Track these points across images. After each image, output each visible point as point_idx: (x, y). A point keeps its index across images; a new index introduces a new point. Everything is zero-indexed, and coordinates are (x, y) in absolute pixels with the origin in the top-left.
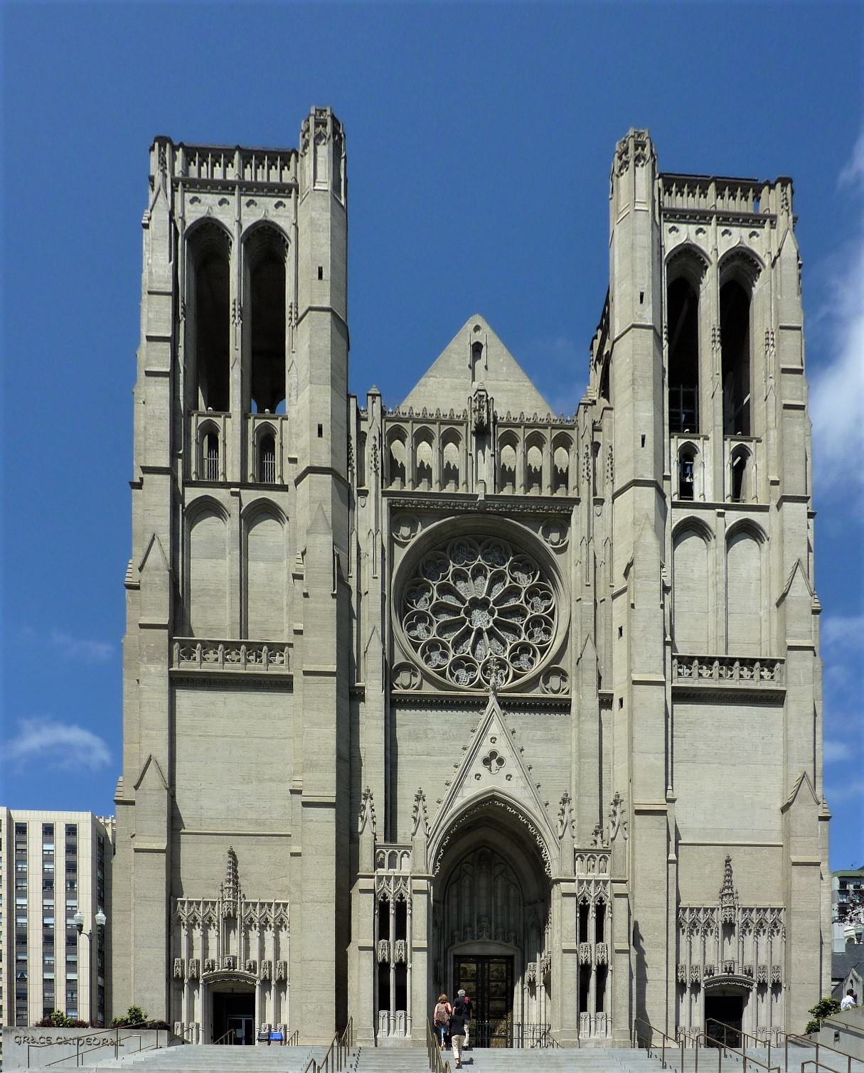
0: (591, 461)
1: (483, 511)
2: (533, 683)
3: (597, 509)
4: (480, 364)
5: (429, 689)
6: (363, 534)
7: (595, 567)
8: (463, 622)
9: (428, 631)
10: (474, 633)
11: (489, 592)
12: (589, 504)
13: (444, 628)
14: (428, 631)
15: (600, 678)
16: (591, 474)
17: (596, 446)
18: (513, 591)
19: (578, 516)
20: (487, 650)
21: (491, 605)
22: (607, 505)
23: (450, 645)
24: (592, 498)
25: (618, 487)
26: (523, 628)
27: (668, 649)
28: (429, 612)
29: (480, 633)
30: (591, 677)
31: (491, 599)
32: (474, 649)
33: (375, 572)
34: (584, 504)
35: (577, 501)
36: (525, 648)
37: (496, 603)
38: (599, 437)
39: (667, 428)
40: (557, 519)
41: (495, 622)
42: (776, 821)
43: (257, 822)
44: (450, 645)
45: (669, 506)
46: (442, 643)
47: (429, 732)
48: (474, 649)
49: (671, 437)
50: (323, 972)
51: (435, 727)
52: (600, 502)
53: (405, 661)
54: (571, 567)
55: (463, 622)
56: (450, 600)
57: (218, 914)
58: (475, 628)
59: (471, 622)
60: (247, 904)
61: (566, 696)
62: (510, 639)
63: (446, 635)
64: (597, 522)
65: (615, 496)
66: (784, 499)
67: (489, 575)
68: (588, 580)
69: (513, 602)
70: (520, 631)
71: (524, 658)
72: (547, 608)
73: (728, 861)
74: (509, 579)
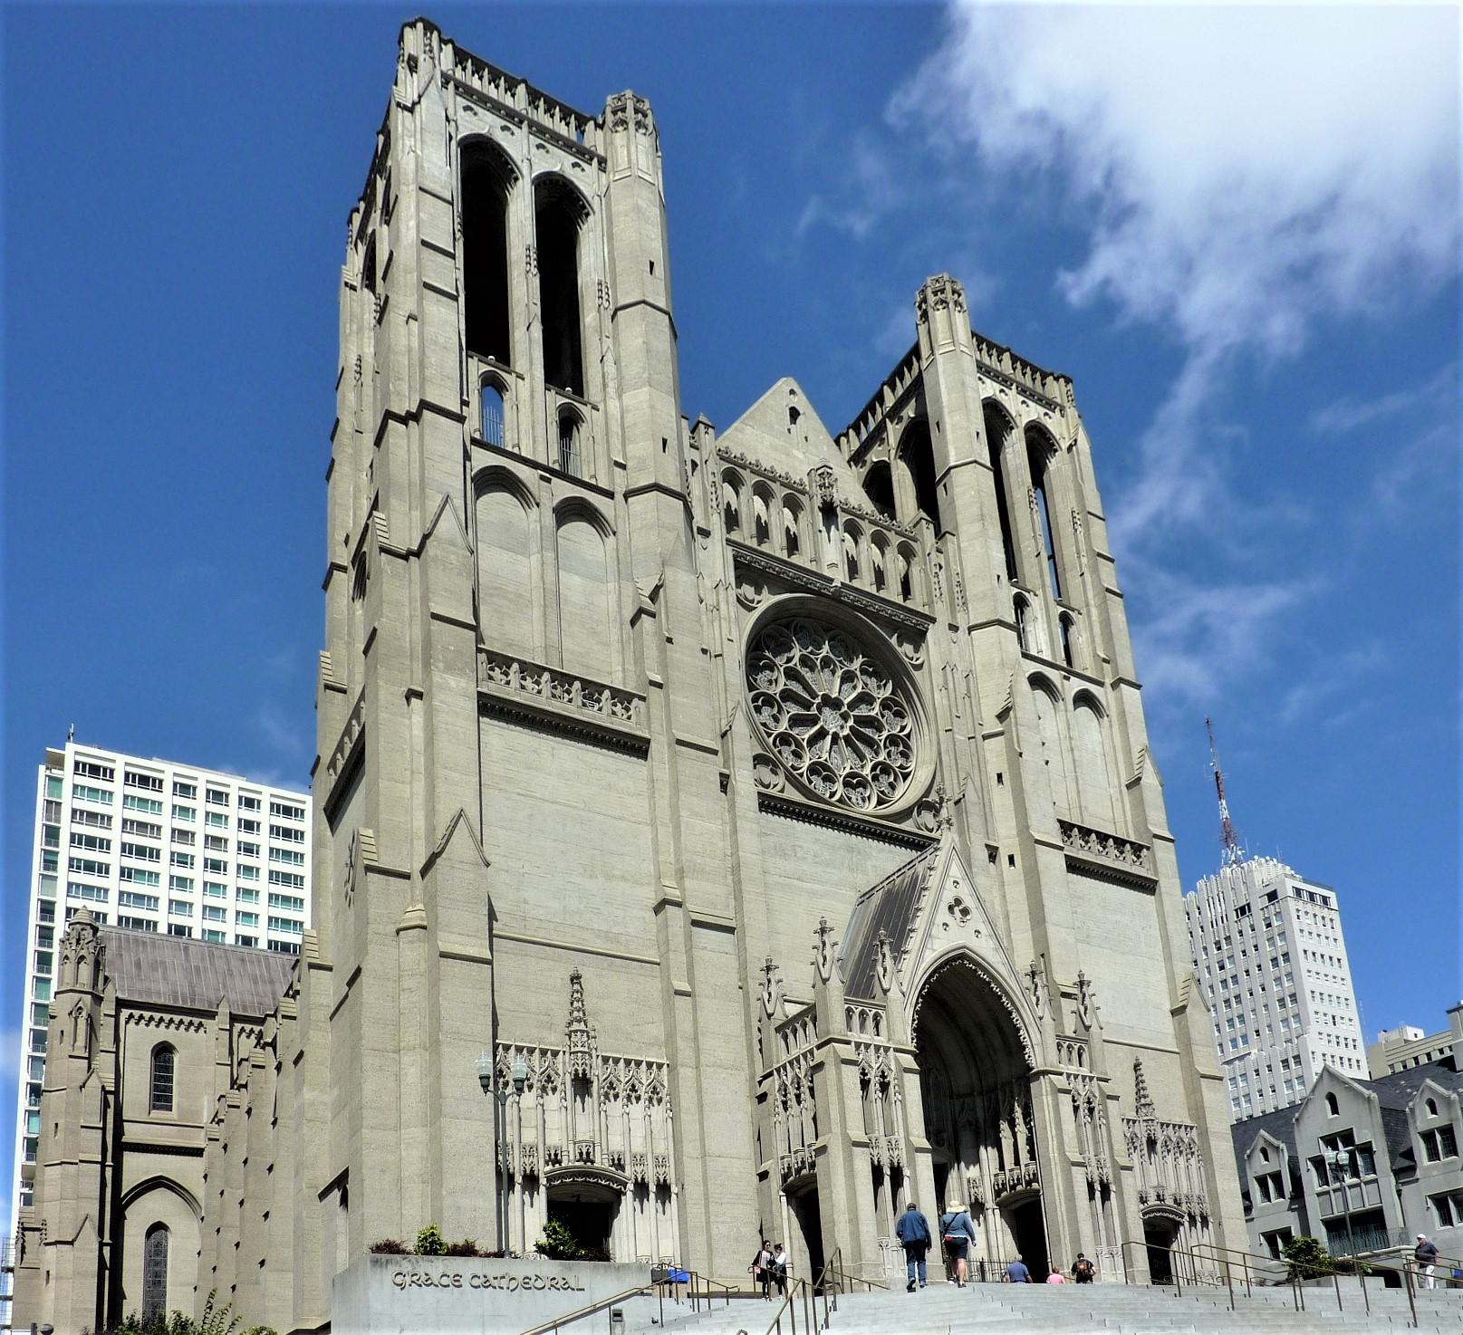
2: (905, 814)
5: (792, 794)
9: (777, 720)
10: (829, 738)
13: (796, 721)
14: (777, 720)
18: (865, 699)
20: (844, 763)
21: (845, 709)
23: (805, 744)
26: (882, 744)
28: (777, 697)
31: (846, 702)
42: (1168, 1024)
43: (607, 936)
44: (805, 744)
46: (795, 740)
47: (798, 850)
50: (736, 1175)
51: (805, 845)
53: (761, 752)
56: (795, 687)
57: (564, 1069)
58: (831, 732)
60: (606, 1060)
70: (879, 746)
73: (1137, 1067)
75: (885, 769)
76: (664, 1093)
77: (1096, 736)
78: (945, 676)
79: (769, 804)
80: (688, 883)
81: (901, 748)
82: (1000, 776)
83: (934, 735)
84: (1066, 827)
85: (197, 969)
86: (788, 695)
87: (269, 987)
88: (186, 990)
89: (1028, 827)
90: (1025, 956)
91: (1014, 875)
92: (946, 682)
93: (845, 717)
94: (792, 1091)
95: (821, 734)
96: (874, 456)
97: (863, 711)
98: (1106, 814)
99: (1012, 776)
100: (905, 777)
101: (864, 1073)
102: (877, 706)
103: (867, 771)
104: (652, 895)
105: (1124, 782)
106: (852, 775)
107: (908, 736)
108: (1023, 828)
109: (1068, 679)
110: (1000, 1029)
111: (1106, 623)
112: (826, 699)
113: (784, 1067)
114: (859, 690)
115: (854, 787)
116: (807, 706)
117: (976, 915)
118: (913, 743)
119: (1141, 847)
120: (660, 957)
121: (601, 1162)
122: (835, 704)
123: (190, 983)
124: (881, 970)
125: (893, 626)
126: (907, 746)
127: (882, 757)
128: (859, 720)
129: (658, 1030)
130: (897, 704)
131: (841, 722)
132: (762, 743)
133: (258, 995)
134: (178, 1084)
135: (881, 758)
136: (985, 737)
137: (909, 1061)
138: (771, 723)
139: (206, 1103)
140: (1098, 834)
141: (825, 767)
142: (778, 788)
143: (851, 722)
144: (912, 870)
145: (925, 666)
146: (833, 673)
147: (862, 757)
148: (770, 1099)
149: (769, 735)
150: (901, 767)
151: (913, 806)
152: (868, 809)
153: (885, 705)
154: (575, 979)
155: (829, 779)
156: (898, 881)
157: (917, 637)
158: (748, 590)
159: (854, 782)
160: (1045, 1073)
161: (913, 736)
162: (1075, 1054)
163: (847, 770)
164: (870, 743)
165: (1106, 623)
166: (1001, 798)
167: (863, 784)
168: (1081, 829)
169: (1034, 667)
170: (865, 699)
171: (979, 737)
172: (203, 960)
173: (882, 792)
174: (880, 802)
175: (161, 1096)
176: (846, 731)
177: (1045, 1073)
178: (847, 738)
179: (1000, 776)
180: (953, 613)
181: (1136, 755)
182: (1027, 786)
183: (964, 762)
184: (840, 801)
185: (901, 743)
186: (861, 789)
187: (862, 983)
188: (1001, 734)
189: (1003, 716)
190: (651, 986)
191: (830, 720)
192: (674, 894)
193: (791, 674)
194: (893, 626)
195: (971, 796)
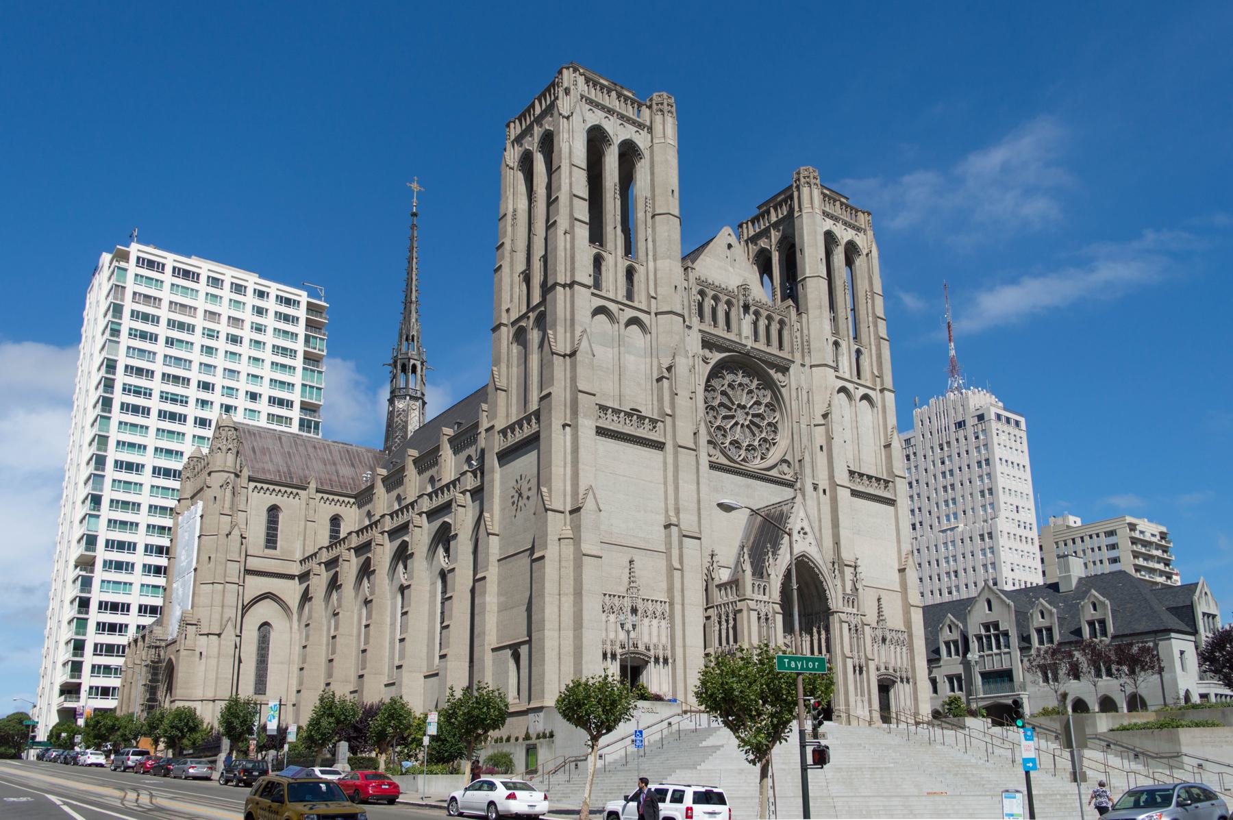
9: (715, 417)
10: (739, 426)
41: (751, 421)
58: (741, 423)
60: (643, 600)
75: (765, 440)
76: (666, 615)
77: (870, 417)
78: (798, 393)
79: (714, 466)
80: (681, 516)
81: (773, 429)
82: (821, 447)
83: (790, 424)
84: (852, 473)
85: (289, 453)
86: (721, 404)
87: (333, 467)
88: (286, 470)
89: (833, 477)
90: (830, 556)
91: (825, 500)
92: (798, 397)
93: (747, 414)
94: (724, 618)
95: (736, 424)
96: (763, 243)
98: (872, 464)
99: (828, 448)
100: (774, 444)
101: (759, 614)
102: (763, 407)
103: (756, 443)
104: (664, 519)
105: (883, 444)
106: (749, 446)
107: (776, 422)
108: (831, 477)
109: (858, 389)
110: (816, 587)
111: (879, 356)
112: (739, 406)
113: (720, 605)
114: (755, 399)
116: (730, 409)
117: (810, 535)
118: (779, 426)
119: (887, 482)
120: (666, 549)
121: (641, 648)
122: (744, 407)
123: (287, 464)
124: (767, 564)
125: (772, 365)
126: (776, 428)
128: (754, 416)
129: (664, 585)
130: (772, 405)
131: (745, 416)
132: (709, 433)
133: (328, 473)
134: (282, 532)
135: (763, 436)
136: (815, 425)
137: (778, 608)
138: (713, 420)
139: (299, 546)
140: (868, 476)
141: (736, 442)
142: (716, 457)
143: (750, 417)
144: (780, 508)
145: (788, 386)
146: (743, 390)
147: (754, 435)
148: (712, 619)
149: (712, 427)
150: (773, 439)
152: (756, 464)
154: (631, 562)
155: (739, 448)
156: (773, 511)
157: (784, 370)
158: (707, 352)
159: (751, 448)
160: (836, 612)
161: (779, 423)
162: (851, 602)
163: (747, 443)
164: (758, 426)
165: (879, 356)
166: (822, 459)
167: (754, 449)
168: (859, 474)
169: (841, 383)
170: (758, 403)
171: (812, 425)
172: (291, 447)
173: (763, 453)
174: (762, 459)
175: (271, 541)
176: (748, 422)
177: (836, 612)
178: (748, 426)
179: (821, 447)
180: (803, 356)
181: (889, 430)
182: (835, 455)
183: (804, 440)
184: (743, 460)
185: (774, 427)
186: (753, 452)
187: (759, 572)
188: (824, 425)
189: (825, 416)
190: (662, 563)
191: (740, 417)
192: (674, 520)
193: (724, 393)
194: (772, 365)
195: (807, 458)
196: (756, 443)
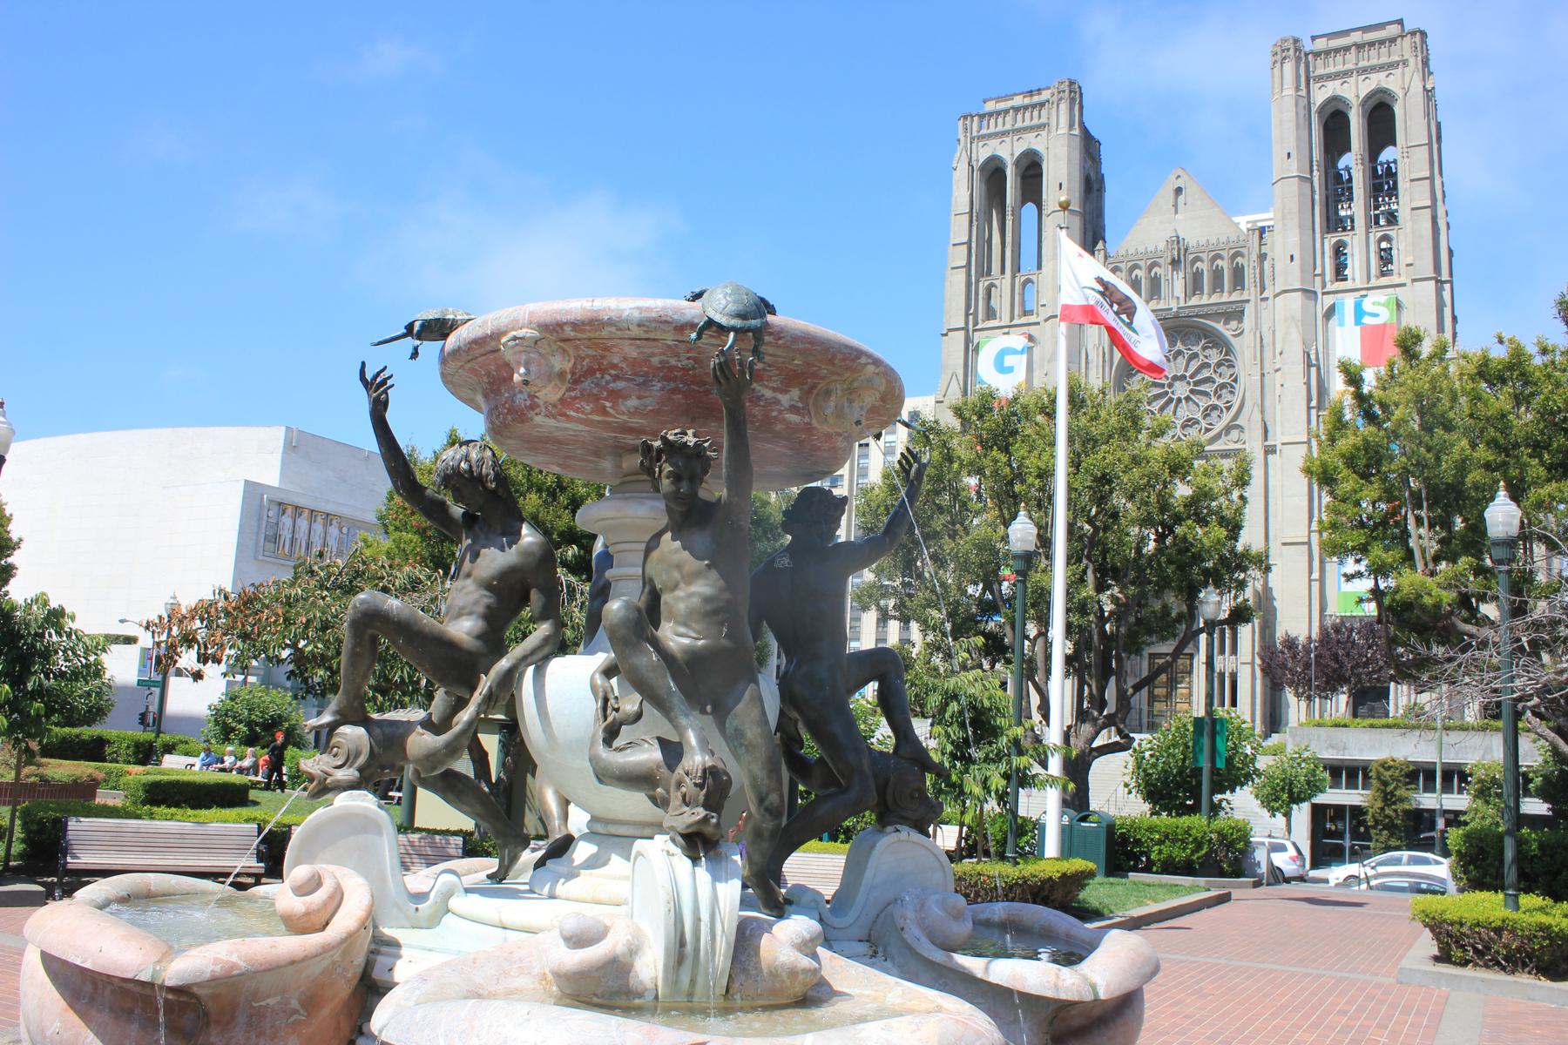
0: (1258, 270)
1: (1176, 317)
2: (1218, 437)
3: (1264, 304)
4: (1181, 199)
6: (1090, 347)
7: (1262, 346)
8: (1167, 393)
11: (1186, 370)
12: (1256, 303)
15: (1266, 431)
16: (1258, 280)
17: (1262, 257)
19: (1249, 310)
22: (1270, 300)
24: (1259, 297)
25: (1277, 291)
27: (1314, 412)
29: (1179, 400)
30: (1259, 433)
31: (1188, 374)
32: (1175, 413)
33: (1098, 373)
34: (1252, 304)
35: (1248, 301)
36: (1214, 407)
37: (1191, 377)
38: (1264, 250)
39: (1318, 236)
40: (1234, 314)
41: (1192, 391)
45: (1320, 295)
48: (1175, 413)
49: (1323, 239)
52: (1266, 299)
54: (1244, 348)
55: (1167, 393)
58: (1175, 397)
59: (1173, 393)
61: (1244, 446)
62: (1203, 403)
63: (1154, 404)
64: (1265, 314)
65: (1275, 296)
66: (1414, 280)
67: (1186, 356)
68: (1255, 360)
69: (1205, 374)
71: (1215, 414)
72: (1231, 375)
74: (1201, 357)
95: (1171, 400)
97: (1205, 374)
100: (1228, 409)
103: (1199, 416)
112: (1175, 378)
115: (1191, 426)
122: (1183, 378)
127: (1214, 401)
128: (1196, 384)
135: (1211, 403)
151: (1221, 432)
153: (1219, 364)
170: (1205, 366)
173: (1211, 424)
176: (1188, 393)
178: (1188, 399)
185: (1230, 387)
191: (1181, 390)
196: (1199, 416)
